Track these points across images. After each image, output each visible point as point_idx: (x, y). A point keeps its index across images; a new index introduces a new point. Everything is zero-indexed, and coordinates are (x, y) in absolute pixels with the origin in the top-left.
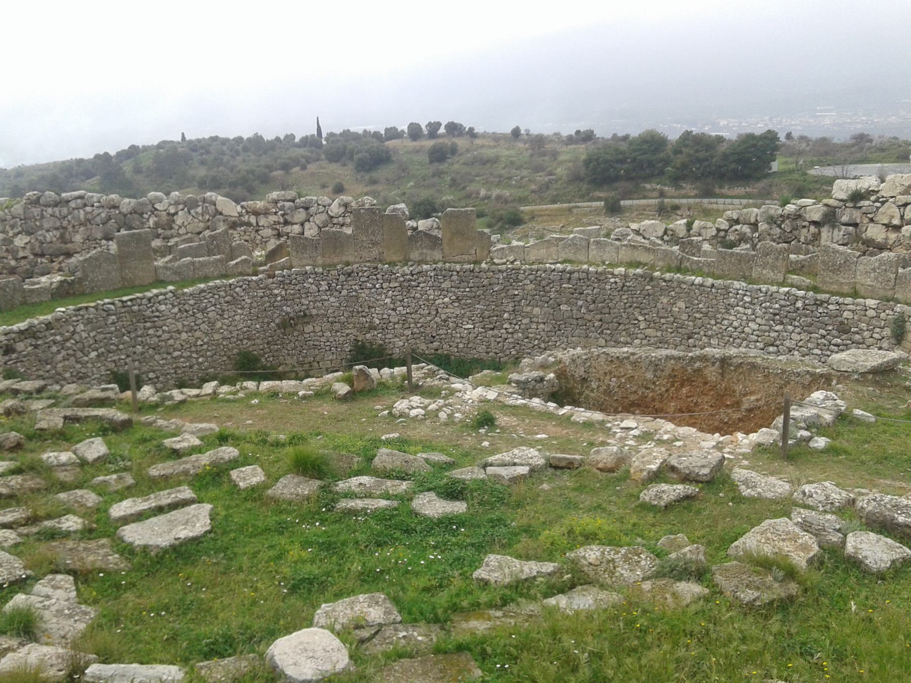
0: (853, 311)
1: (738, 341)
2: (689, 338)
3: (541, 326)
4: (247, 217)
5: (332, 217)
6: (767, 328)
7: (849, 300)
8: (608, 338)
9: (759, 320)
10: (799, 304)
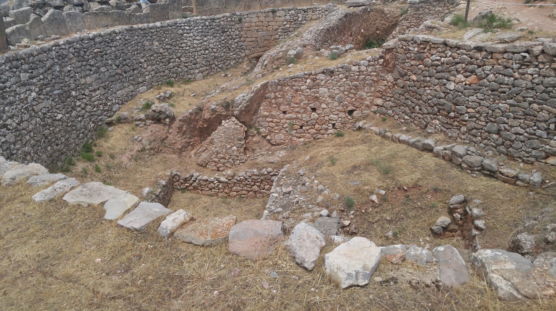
0: (223, 21)
1: (193, 53)
2: (169, 63)
3: (98, 92)
6: (201, 41)
8: (133, 83)
9: (197, 38)
10: (207, 24)
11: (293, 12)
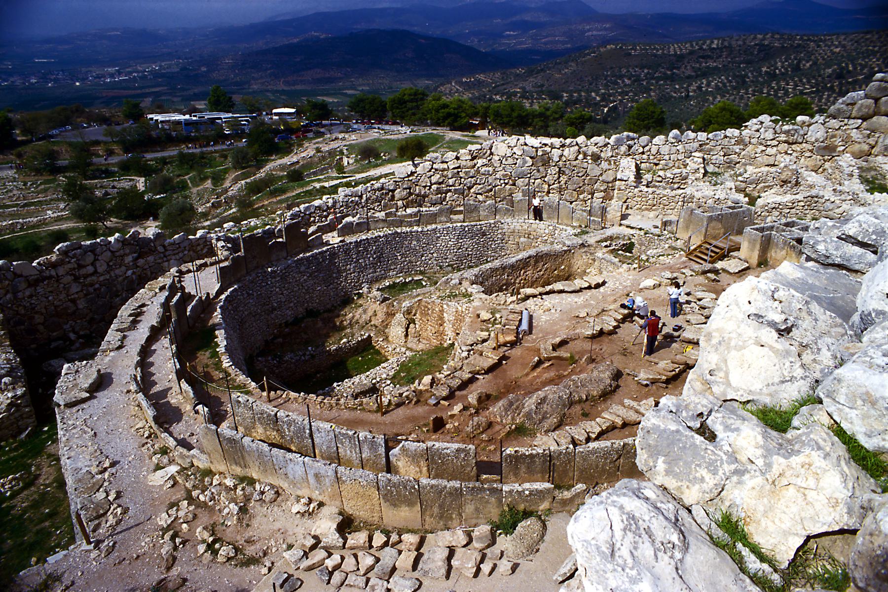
4: (47, 272)
5: (112, 252)
7: (483, 222)
11: (551, 228)
